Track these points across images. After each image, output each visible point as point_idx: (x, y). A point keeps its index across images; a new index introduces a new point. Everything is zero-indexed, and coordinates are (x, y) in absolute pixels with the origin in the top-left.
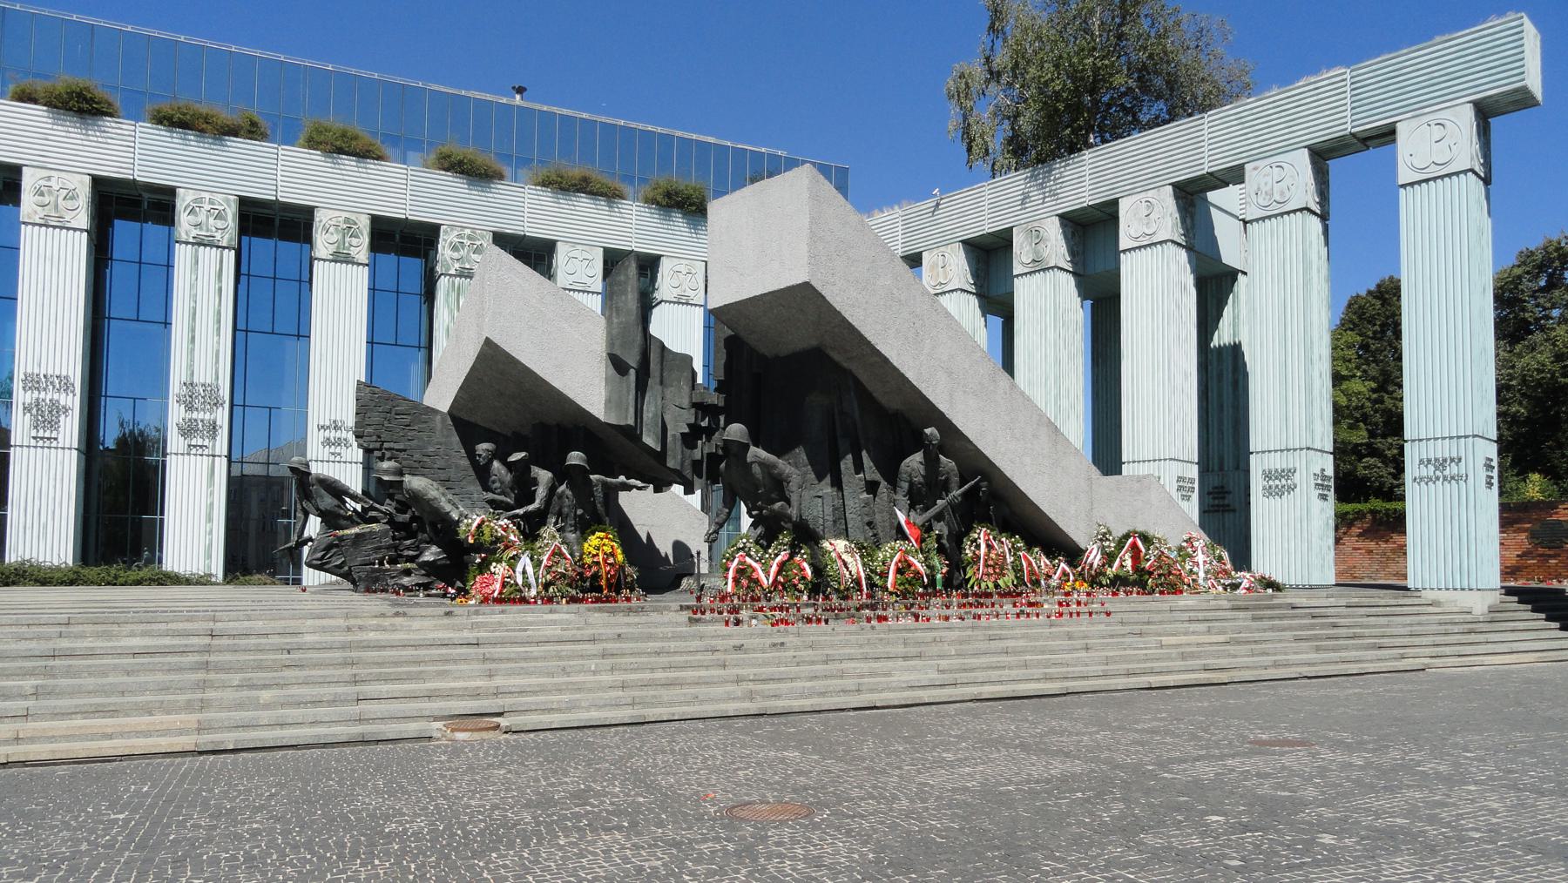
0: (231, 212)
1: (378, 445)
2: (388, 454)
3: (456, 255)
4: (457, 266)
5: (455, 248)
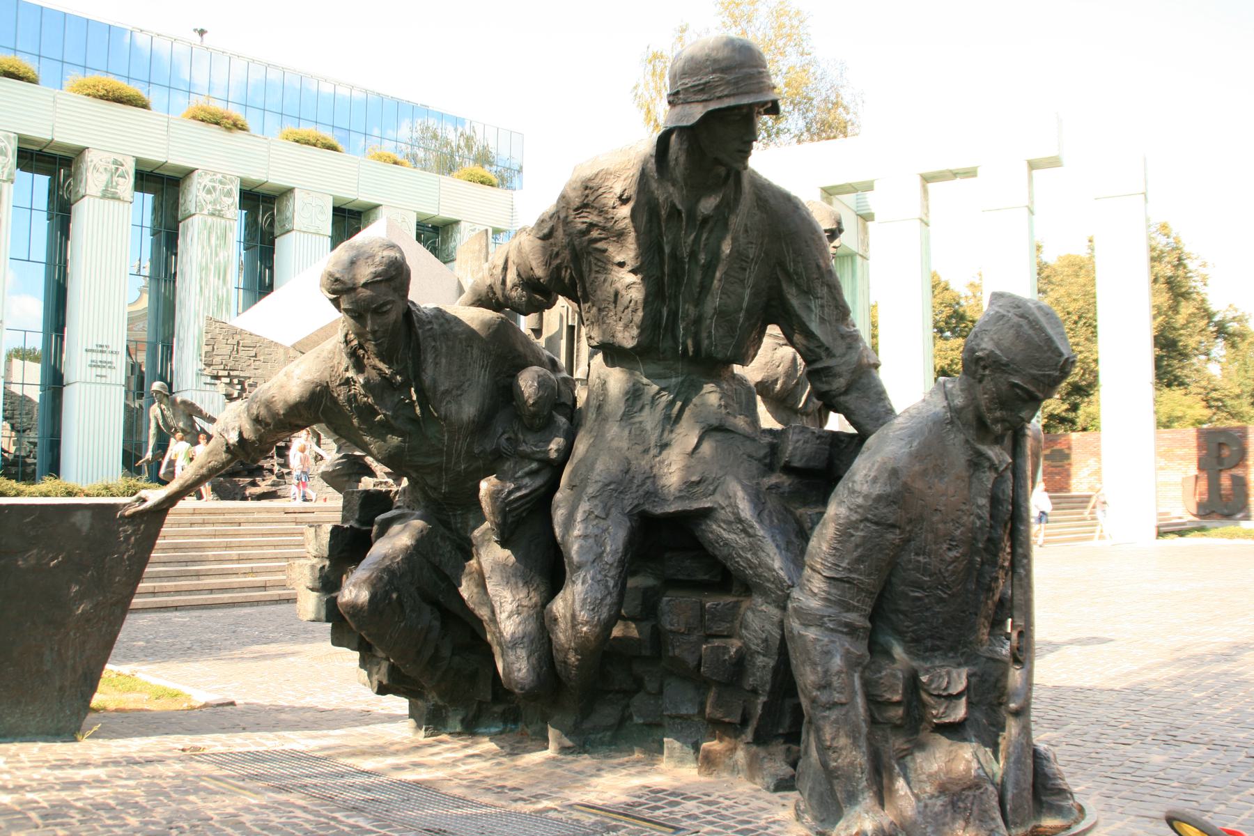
0: (12, 148)
1: (226, 373)
2: (236, 381)
5: (209, 192)
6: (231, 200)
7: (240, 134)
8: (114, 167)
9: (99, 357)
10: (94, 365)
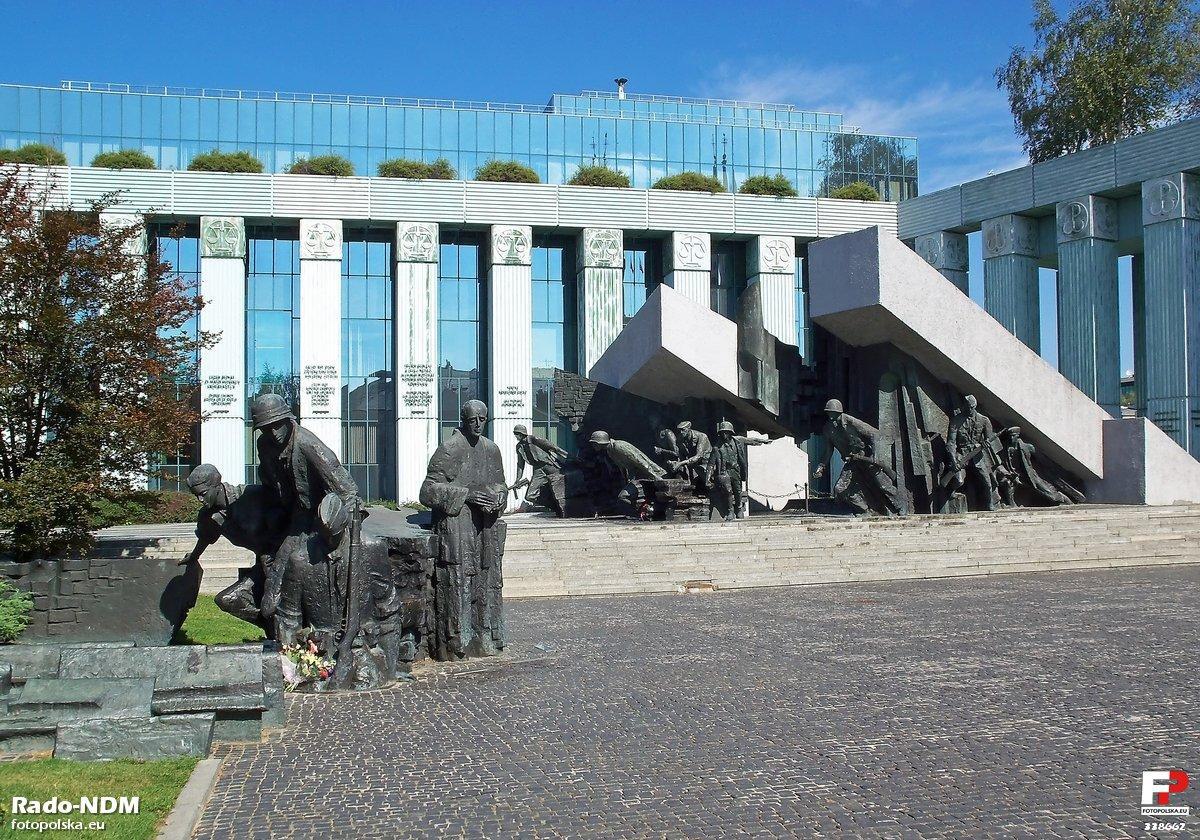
0: (435, 233)
3: (596, 251)
4: (597, 259)
5: (597, 246)
6: (613, 251)
7: (623, 191)
8: (513, 237)
9: (512, 397)
10: (506, 404)
